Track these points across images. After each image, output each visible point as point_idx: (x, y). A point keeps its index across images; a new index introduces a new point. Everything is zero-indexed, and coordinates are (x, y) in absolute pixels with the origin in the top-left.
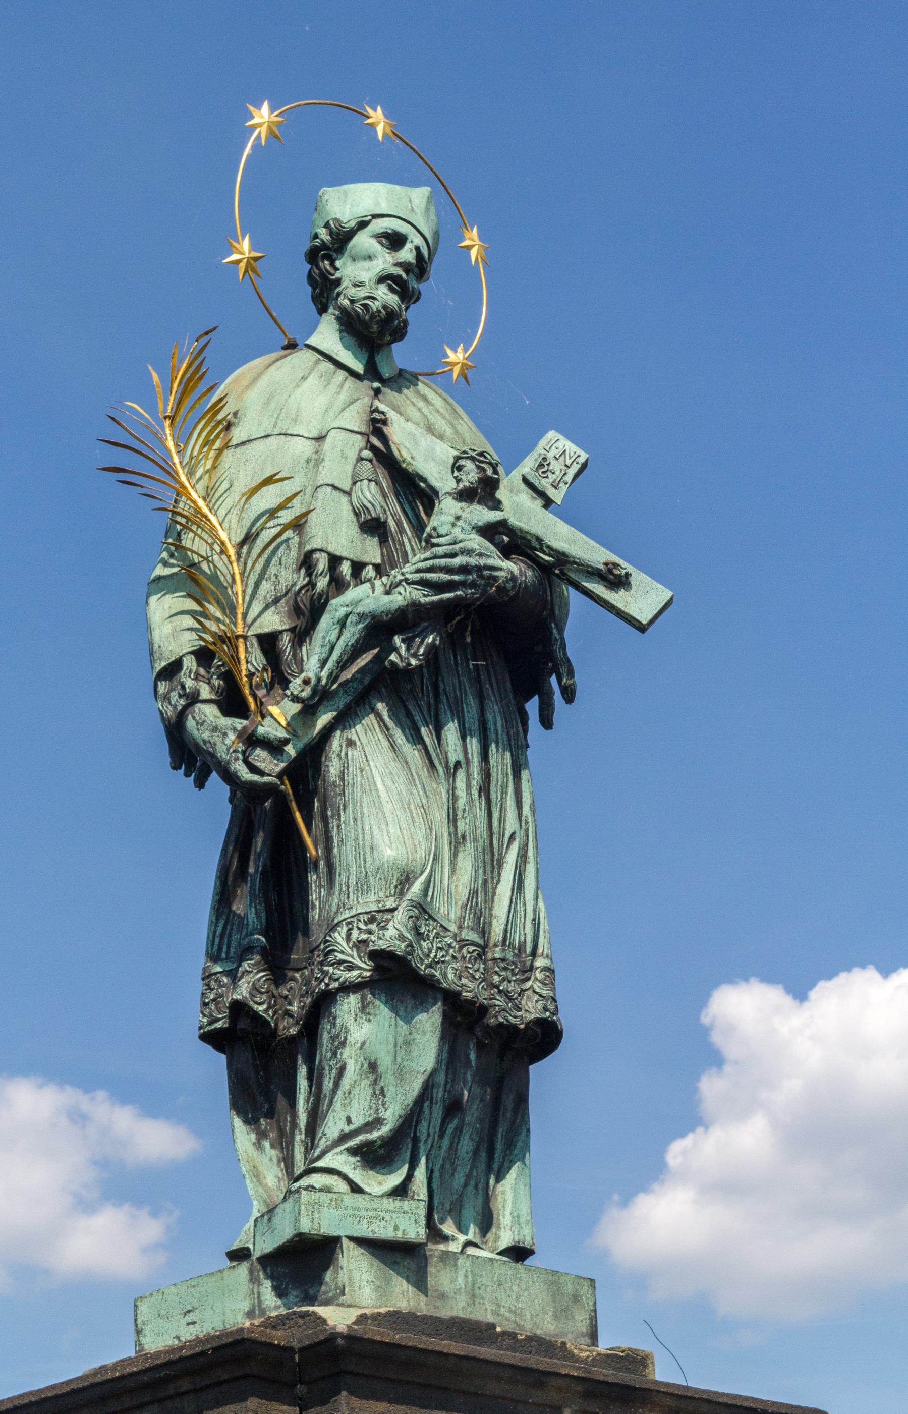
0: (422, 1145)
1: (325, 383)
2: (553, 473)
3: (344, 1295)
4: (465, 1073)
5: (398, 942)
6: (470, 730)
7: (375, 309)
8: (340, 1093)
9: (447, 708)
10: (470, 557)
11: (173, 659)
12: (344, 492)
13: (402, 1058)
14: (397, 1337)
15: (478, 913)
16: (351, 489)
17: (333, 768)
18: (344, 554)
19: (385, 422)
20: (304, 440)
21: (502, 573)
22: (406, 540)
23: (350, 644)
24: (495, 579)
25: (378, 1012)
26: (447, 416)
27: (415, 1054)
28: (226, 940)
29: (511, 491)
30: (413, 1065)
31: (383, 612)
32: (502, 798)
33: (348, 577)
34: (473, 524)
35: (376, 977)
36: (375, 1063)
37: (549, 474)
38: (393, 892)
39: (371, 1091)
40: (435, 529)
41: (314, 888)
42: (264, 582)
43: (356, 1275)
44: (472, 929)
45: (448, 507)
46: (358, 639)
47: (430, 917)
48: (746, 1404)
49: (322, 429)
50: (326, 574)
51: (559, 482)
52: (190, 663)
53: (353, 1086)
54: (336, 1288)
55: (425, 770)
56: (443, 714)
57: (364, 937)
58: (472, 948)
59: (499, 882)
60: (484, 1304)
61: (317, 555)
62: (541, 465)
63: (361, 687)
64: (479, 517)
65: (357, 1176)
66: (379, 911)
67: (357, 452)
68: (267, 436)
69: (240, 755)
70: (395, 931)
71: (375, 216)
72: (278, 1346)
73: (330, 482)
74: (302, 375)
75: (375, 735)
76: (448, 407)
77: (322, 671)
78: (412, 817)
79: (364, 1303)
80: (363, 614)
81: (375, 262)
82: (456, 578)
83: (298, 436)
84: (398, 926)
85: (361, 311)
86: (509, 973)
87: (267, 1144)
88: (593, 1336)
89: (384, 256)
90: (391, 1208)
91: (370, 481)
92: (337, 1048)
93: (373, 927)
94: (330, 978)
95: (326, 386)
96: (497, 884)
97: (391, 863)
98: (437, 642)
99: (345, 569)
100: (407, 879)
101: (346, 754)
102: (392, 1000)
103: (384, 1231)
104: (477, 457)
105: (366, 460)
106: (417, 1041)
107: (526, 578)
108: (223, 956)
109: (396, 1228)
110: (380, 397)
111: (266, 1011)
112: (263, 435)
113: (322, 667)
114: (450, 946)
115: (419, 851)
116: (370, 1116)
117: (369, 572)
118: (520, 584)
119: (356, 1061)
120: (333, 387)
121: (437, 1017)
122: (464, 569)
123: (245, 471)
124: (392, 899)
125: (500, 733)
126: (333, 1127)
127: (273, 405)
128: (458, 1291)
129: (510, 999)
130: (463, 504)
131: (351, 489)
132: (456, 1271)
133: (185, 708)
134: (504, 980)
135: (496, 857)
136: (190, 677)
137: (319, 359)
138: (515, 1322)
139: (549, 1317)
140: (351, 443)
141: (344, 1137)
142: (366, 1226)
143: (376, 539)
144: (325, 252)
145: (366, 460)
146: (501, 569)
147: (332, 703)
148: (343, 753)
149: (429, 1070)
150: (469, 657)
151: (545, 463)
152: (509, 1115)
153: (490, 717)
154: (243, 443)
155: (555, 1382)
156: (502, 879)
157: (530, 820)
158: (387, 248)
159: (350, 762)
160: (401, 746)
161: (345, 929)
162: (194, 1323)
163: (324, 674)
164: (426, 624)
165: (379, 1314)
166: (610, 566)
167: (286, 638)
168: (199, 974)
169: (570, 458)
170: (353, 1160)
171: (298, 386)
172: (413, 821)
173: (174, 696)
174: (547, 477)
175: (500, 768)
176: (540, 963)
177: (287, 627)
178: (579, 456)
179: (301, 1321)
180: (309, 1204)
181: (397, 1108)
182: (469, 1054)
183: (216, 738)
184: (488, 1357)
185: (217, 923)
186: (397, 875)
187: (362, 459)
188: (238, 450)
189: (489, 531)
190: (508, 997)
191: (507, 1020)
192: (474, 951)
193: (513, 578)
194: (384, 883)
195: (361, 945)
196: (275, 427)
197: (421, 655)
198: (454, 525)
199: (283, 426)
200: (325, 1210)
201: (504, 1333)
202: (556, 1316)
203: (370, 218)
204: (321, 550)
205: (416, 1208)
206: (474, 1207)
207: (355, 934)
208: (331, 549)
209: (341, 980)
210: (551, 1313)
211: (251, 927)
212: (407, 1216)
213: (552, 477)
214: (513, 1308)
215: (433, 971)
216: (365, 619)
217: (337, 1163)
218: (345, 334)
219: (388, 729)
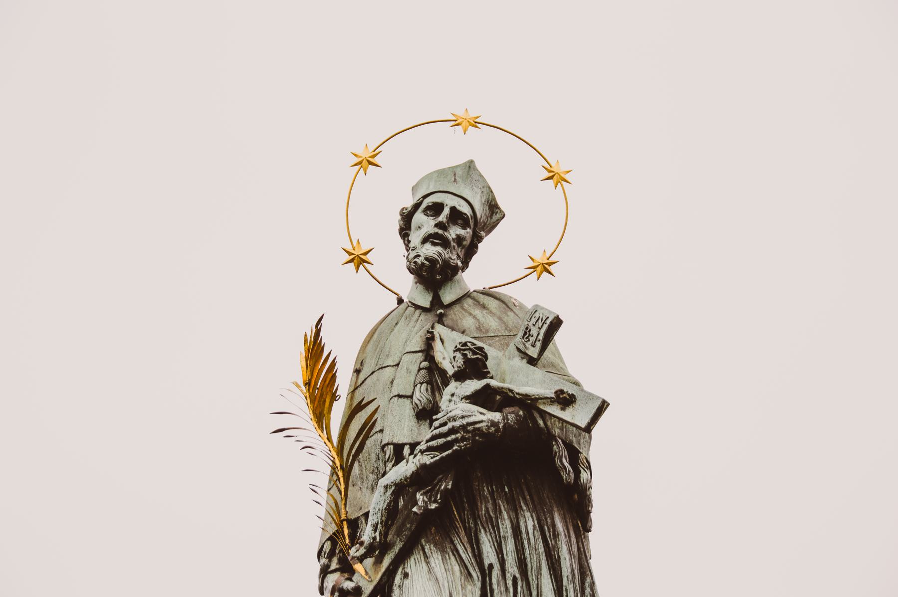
2: (532, 336)
6: (505, 537)
7: (420, 263)
9: (481, 527)
10: (455, 421)
18: (404, 442)
21: (483, 424)
23: (384, 508)
24: (479, 429)
31: (401, 479)
45: (453, 386)
46: (390, 502)
52: (328, 547)
55: (463, 578)
56: (479, 532)
62: (525, 333)
73: (396, 394)
74: (396, 322)
75: (421, 564)
80: (387, 485)
81: (422, 230)
82: (449, 439)
83: (388, 366)
85: (414, 267)
91: (421, 383)
95: (408, 324)
98: (449, 487)
99: (406, 451)
105: (423, 369)
110: (444, 319)
112: (371, 373)
113: (375, 531)
120: (412, 324)
122: (453, 431)
125: (531, 531)
137: (409, 306)
147: (392, 550)
150: (504, 483)
153: (522, 523)
154: (363, 382)
158: (431, 216)
160: (434, 568)
163: (377, 534)
164: (441, 476)
169: (542, 320)
174: (529, 340)
178: (548, 318)
189: (474, 398)
193: (494, 424)
197: (439, 500)
198: (450, 401)
204: (388, 444)
208: (395, 441)
213: (532, 339)
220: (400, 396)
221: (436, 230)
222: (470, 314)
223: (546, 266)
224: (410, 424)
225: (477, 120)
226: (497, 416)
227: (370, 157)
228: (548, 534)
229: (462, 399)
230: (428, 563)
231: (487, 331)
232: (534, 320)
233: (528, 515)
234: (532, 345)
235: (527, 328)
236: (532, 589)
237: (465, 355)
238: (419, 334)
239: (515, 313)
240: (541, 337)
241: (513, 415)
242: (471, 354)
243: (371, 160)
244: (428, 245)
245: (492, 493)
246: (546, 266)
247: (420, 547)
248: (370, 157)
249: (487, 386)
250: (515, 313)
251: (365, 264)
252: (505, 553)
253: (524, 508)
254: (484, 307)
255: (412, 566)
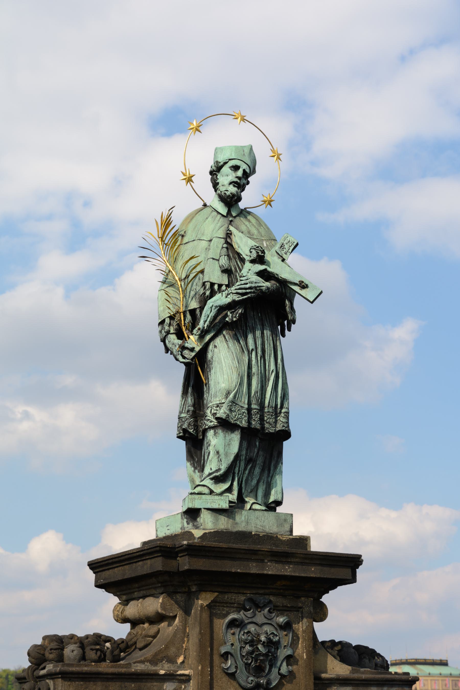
0: (236, 475)
1: (214, 220)
3: (202, 526)
4: (255, 449)
5: (223, 415)
6: (258, 337)
8: (208, 461)
11: (163, 319)
12: (217, 260)
13: (227, 449)
14: (204, 544)
15: (258, 398)
16: (219, 258)
17: (209, 355)
18: (216, 282)
19: (231, 234)
20: (205, 241)
22: (237, 274)
23: (213, 316)
24: (261, 290)
25: (219, 436)
26: (257, 226)
27: (231, 448)
28: (185, 406)
29: (272, 256)
30: (231, 451)
31: (223, 305)
32: (269, 358)
33: (216, 290)
34: (254, 272)
35: (218, 425)
36: (218, 451)
37: (284, 249)
38: (224, 397)
39: (217, 460)
40: (242, 274)
41: (205, 393)
42: (192, 291)
43: (206, 520)
44: (255, 404)
45: (248, 265)
47: (236, 404)
48: (330, 555)
49: (211, 237)
50: (209, 290)
51: (287, 252)
52: (167, 321)
53: (212, 459)
54: (200, 524)
57: (215, 412)
58: (255, 410)
59: (268, 386)
60: (251, 525)
61: (206, 284)
62: (281, 246)
63: (219, 328)
64: (257, 269)
65: (213, 487)
66: (220, 403)
67: (222, 245)
68: (194, 240)
69: (180, 353)
70: (223, 411)
71: (230, 160)
72: (169, 547)
74: (206, 217)
76: (258, 222)
77: (205, 324)
78: (232, 371)
79: (209, 528)
81: (229, 177)
82: (248, 291)
84: (224, 409)
86: (270, 416)
87: (197, 471)
88: (291, 531)
89: (232, 175)
90: (218, 499)
91: (225, 255)
92: (208, 446)
93: (218, 408)
94: (206, 425)
95: (214, 221)
96: (267, 387)
97: (224, 388)
98: (243, 312)
99: (216, 287)
100: (229, 393)
101: (214, 350)
102: (224, 431)
103: (216, 506)
104: (256, 248)
105: (225, 248)
106: (232, 444)
107: (273, 287)
108: (184, 412)
109: (219, 505)
110: (232, 223)
111: (193, 431)
112: (193, 240)
114: (244, 412)
115: (233, 383)
116: (217, 468)
117: (224, 288)
118: (271, 290)
119: (213, 451)
120: (216, 221)
121: (239, 436)
122: (250, 288)
123: (187, 253)
124: (224, 399)
125: (269, 337)
126: (207, 471)
127: (196, 229)
128: (243, 521)
129: (271, 424)
130: (252, 265)
131: (219, 258)
132: (242, 515)
133: (166, 336)
134: (268, 418)
135: (267, 378)
136: (167, 325)
138: (263, 529)
139: (275, 527)
140: (220, 242)
141: (210, 474)
142: (209, 505)
143: (227, 275)
144: (214, 173)
145: (225, 248)
146: (263, 286)
148: (213, 350)
149: (236, 453)
150: (259, 312)
151: (283, 246)
152: (275, 458)
154: (187, 243)
155: (260, 552)
156: (269, 385)
157: (280, 364)
159: (215, 353)
161: (210, 409)
162: (169, 529)
163: (206, 326)
165: (211, 532)
166: (301, 282)
167: (198, 311)
168: (177, 418)
169: (291, 243)
170: (212, 481)
171: (205, 221)
172: (233, 373)
173: (163, 331)
174: (283, 250)
175: (269, 348)
176: (283, 410)
177: (198, 306)
178: (294, 242)
179: (188, 534)
180: (191, 499)
181: (225, 465)
182: (256, 443)
183: (173, 347)
184: (236, 547)
185: (182, 401)
186: (225, 392)
187: (224, 247)
188: (185, 245)
190: (269, 424)
191: (269, 431)
192: (255, 411)
194: (221, 394)
195: (214, 414)
196: (196, 237)
198: (248, 272)
199: (199, 237)
200: (196, 500)
201: (255, 534)
202: (278, 526)
203: (228, 160)
204: (208, 282)
205: (226, 498)
206: (262, 489)
207: (212, 411)
208: (211, 281)
209: (208, 425)
210: (276, 526)
211: (189, 404)
212: (223, 501)
214: (262, 525)
215: (236, 422)
216: (217, 308)
217: (206, 483)
218: (220, 202)
219: (227, 341)
220: (213, 259)
221: (236, 180)
222: (244, 224)
223: (270, 202)
224: (218, 274)
225: (245, 118)
226: (268, 284)
227: (197, 127)
228: (274, 339)
229: (254, 273)
230: (227, 344)
231: (253, 235)
232: (286, 241)
233: (268, 328)
234: (285, 253)
235: (283, 244)
236: (266, 362)
237: (258, 253)
238: (222, 229)
239: (264, 228)
240: (290, 251)
241: (275, 286)
242: (261, 253)
243: (197, 128)
244: (231, 186)
245: (254, 315)
246: (270, 202)
247: (222, 335)
248: (197, 127)
249: (266, 269)
250: (264, 228)
251: (191, 183)
252: (258, 344)
253: (267, 325)
254: (249, 221)
255: (218, 343)
